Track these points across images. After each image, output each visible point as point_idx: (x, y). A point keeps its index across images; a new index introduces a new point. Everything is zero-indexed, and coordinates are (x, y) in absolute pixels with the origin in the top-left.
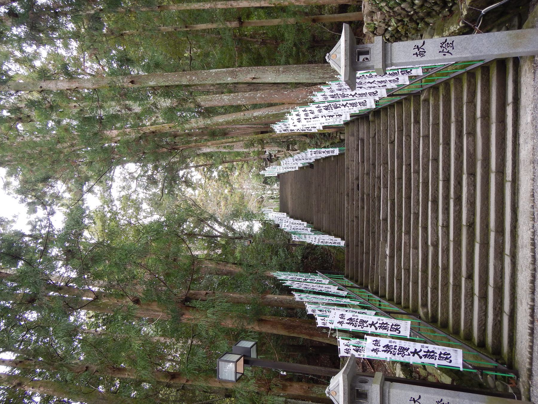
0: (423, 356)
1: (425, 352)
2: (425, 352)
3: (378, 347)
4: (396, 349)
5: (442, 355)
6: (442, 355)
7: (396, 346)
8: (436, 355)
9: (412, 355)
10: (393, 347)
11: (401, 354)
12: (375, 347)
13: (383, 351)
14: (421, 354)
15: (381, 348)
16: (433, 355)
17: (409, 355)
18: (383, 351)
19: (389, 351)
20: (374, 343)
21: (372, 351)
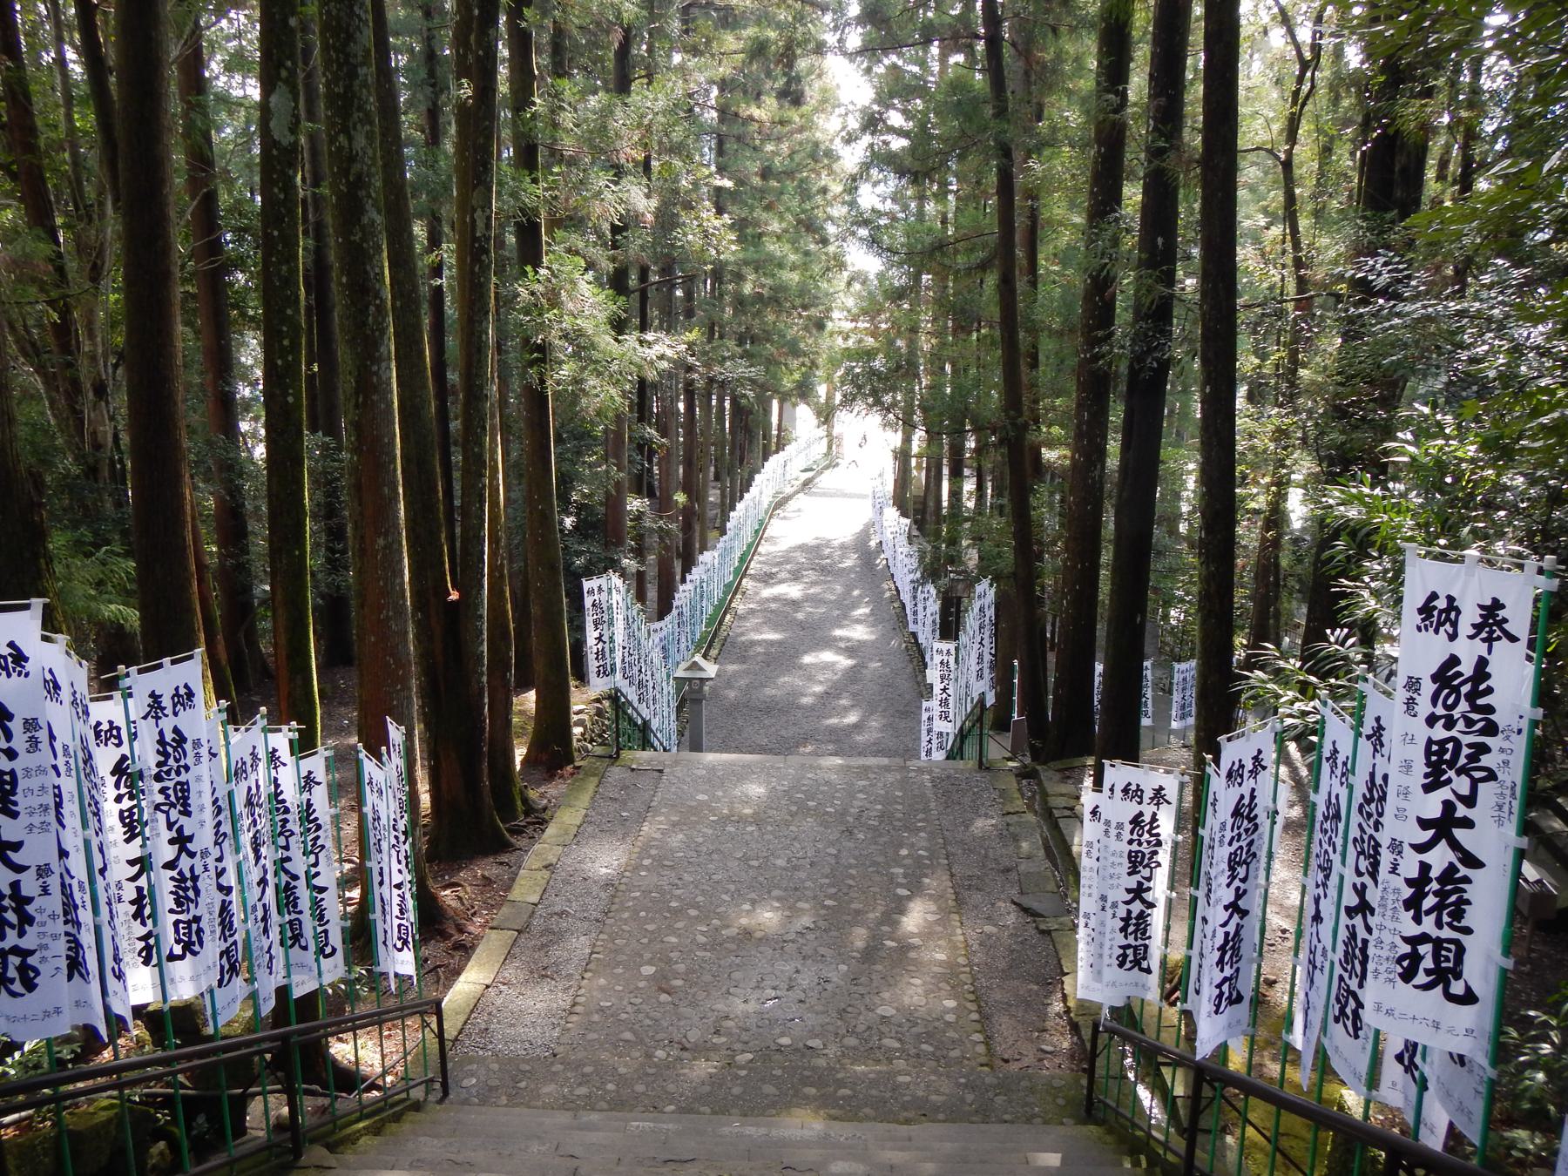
0: (181, 873)
1: (192, 869)
2: (192, 869)
3: (169, 711)
4: (178, 773)
6: (194, 926)
8: (192, 906)
9: (174, 834)
11: (167, 797)
12: (166, 702)
13: (161, 733)
14: (185, 863)
16: (188, 899)
17: (170, 826)
18: (161, 733)
19: (166, 755)
20: (182, 691)
21: (153, 695)
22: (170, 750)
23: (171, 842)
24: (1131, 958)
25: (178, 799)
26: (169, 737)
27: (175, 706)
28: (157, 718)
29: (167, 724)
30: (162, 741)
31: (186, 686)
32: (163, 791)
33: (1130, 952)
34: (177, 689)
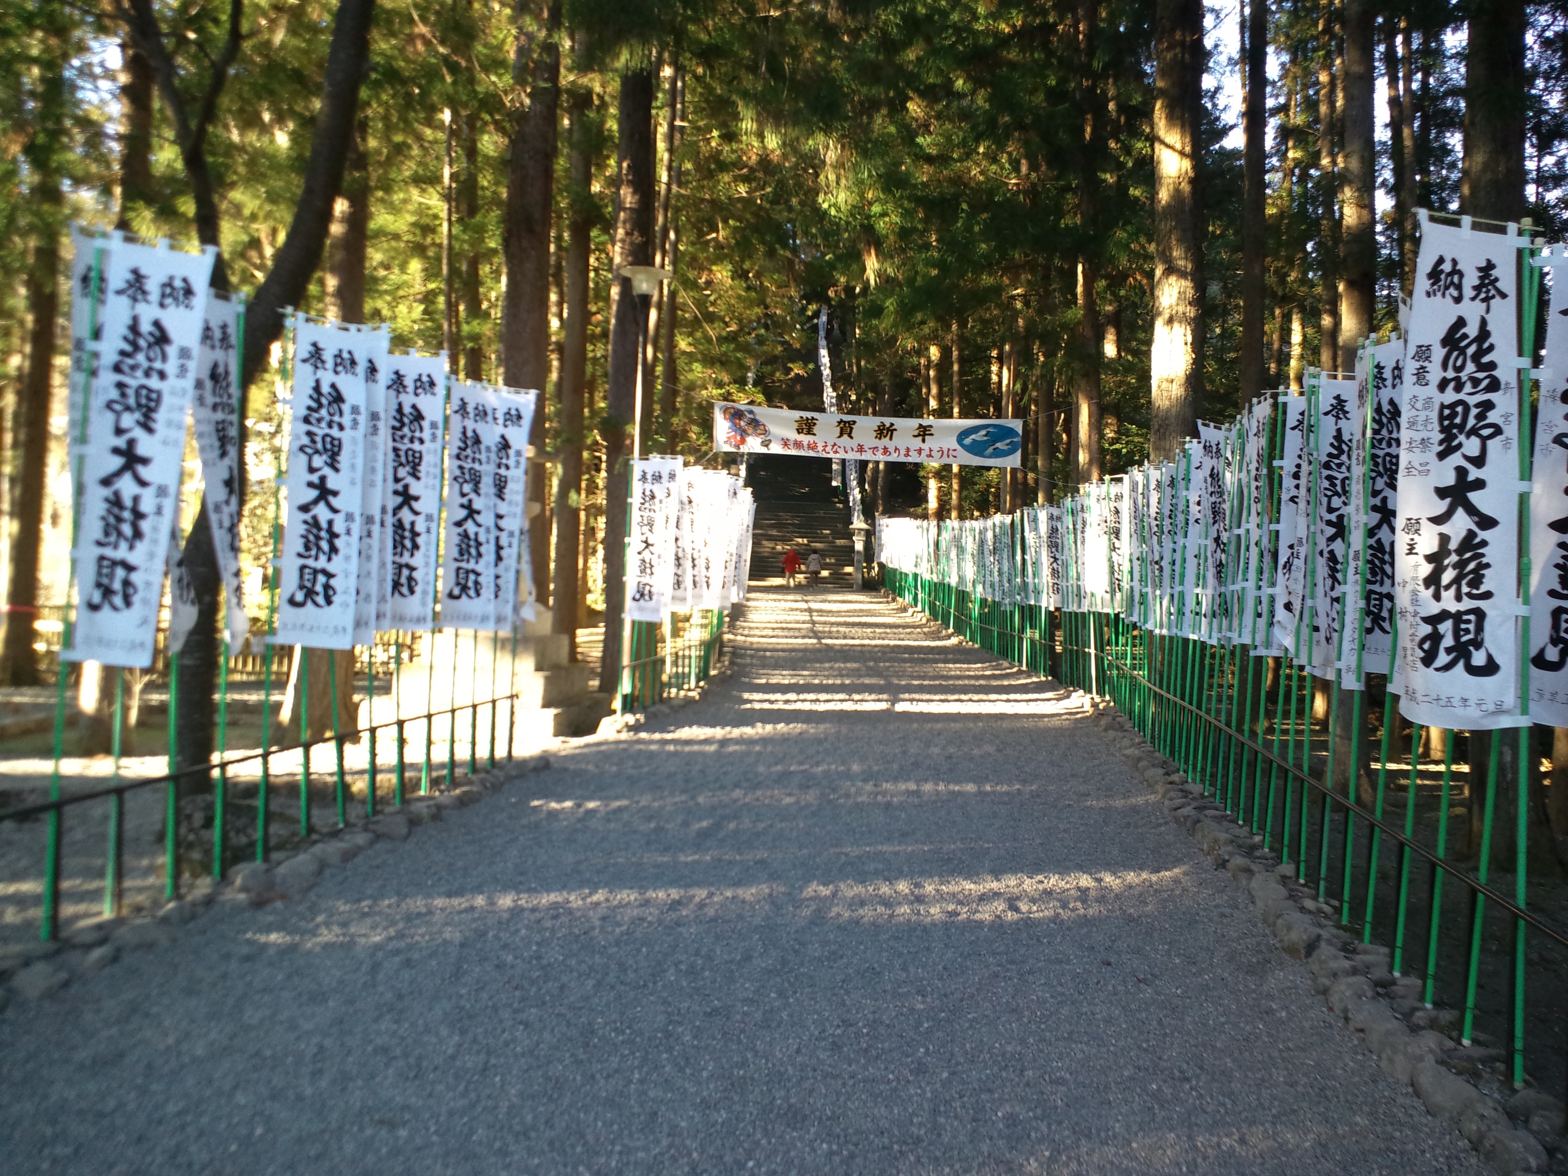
5: (120, 573)
7: (162, 375)
10: (158, 365)
12: (153, 286)
13: (135, 319)
15: (148, 313)
18: (135, 319)
21: (135, 272)
22: (142, 343)
23: (116, 451)
24: (1448, 641)
25: (139, 405)
26: (146, 327)
27: (163, 296)
28: (135, 300)
29: (148, 313)
30: (134, 328)
31: (185, 280)
32: (120, 386)
33: (1447, 627)
34: (171, 278)
